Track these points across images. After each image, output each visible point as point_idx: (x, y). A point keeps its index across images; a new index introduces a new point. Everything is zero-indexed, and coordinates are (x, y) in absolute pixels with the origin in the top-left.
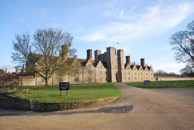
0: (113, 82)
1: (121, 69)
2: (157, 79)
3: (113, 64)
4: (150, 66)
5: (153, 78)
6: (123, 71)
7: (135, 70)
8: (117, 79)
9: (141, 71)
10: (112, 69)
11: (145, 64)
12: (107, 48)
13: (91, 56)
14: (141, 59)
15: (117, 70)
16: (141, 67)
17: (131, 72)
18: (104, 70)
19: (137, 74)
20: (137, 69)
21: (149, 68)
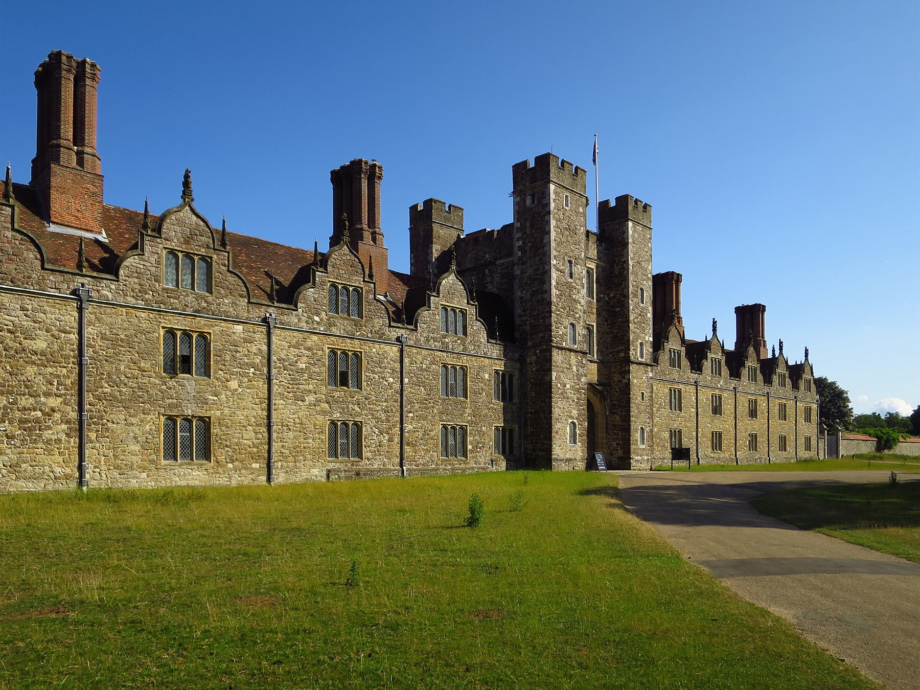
0: (564, 467)
1: (627, 361)
2: (833, 449)
3: (571, 312)
4: (794, 357)
5: (814, 442)
6: (639, 379)
7: (713, 380)
8: (592, 447)
9: (750, 386)
10: (557, 357)
11: (769, 347)
12: (520, 170)
13: (372, 222)
14: (741, 312)
15: (592, 372)
16: (751, 363)
17: (692, 389)
18: (486, 359)
19: (727, 407)
20: (725, 371)
21: (797, 372)
